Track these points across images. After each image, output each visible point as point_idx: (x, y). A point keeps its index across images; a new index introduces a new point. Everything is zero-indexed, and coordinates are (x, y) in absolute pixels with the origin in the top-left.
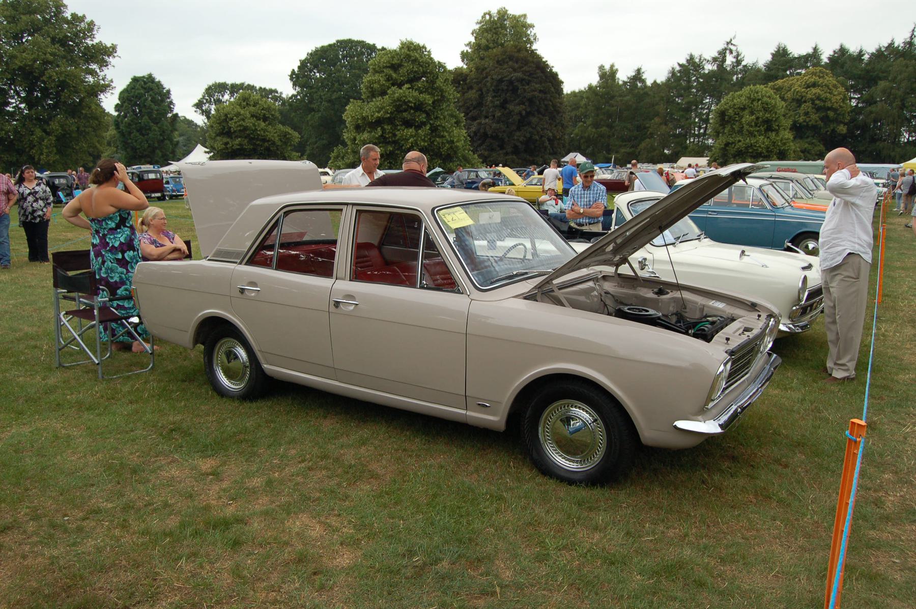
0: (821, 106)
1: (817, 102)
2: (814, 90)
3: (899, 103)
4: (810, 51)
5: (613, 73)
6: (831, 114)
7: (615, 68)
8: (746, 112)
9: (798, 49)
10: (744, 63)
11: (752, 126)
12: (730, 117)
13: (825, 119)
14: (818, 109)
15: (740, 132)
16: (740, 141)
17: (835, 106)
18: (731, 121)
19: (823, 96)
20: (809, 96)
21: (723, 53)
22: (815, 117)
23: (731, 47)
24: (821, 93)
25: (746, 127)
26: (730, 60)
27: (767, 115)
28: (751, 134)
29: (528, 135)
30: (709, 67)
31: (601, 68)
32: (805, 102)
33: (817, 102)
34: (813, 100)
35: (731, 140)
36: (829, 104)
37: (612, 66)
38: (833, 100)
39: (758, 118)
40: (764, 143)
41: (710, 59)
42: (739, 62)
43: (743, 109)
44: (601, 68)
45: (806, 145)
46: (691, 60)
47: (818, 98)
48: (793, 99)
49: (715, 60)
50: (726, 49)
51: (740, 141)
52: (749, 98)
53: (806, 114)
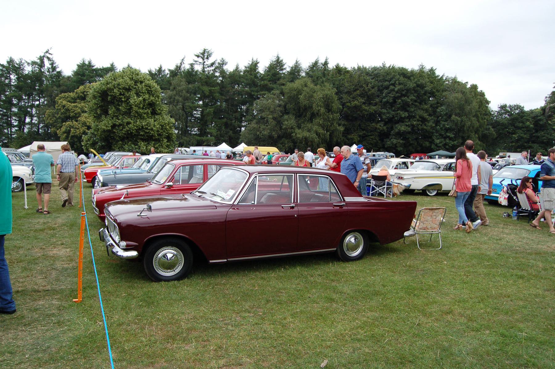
3: (181, 106)
4: (109, 66)
8: (132, 93)
9: (99, 63)
10: (58, 70)
11: (139, 108)
12: (114, 97)
15: (128, 113)
16: (128, 123)
18: (116, 101)
21: (41, 59)
23: (48, 55)
25: (135, 108)
26: (47, 64)
27: (152, 98)
28: (140, 116)
30: (28, 69)
35: (118, 122)
39: (144, 100)
40: (154, 126)
42: (54, 69)
43: (129, 90)
46: (11, 61)
49: (34, 63)
50: (44, 56)
51: (128, 123)
52: (132, 79)
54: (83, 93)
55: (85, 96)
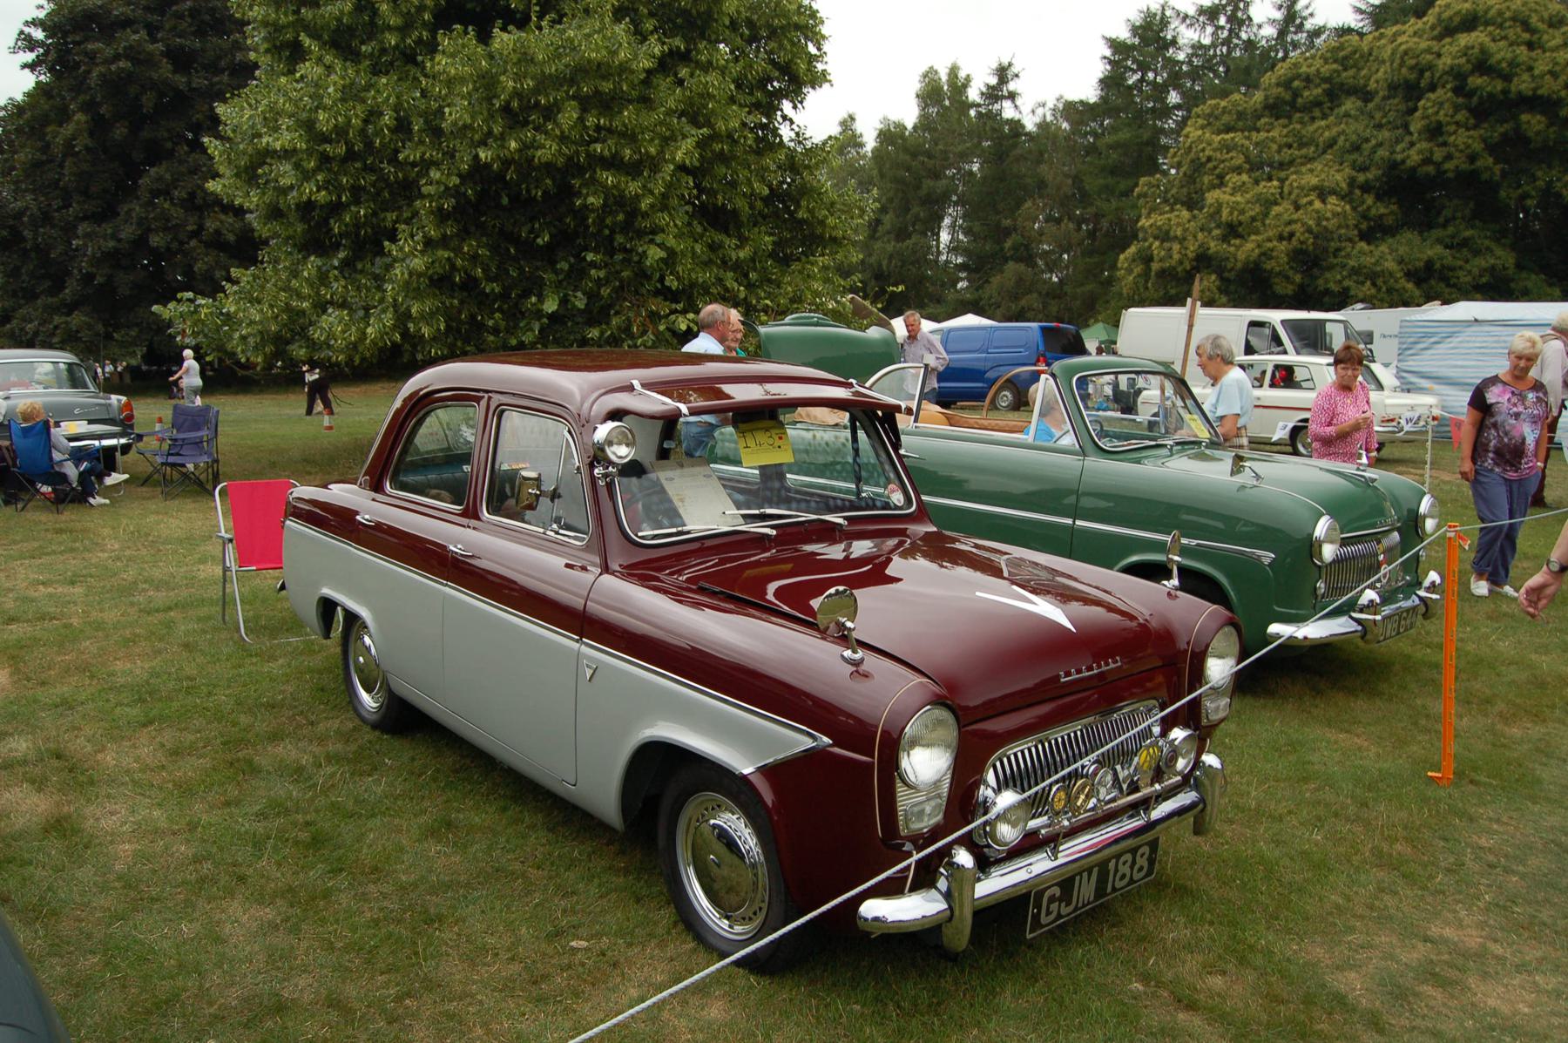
0: (1492, 100)
1: (1476, 81)
2: (1464, 39)
5: (959, 86)
6: (1533, 122)
7: (962, 74)
13: (1514, 148)
14: (1483, 110)
17: (1549, 87)
19: (1501, 53)
20: (1446, 61)
22: (1465, 139)
24: (1493, 47)
29: (128, 232)
31: (930, 76)
32: (1432, 88)
33: (1476, 81)
34: (1459, 78)
36: (1523, 84)
37: (953, 71)
38: (1541, 67)
41: (1192, 11)
44: (930, 76)
45: (1439, 249)
47: (1483, 65)
48: (1393, 88)
53: (1434, 131)
54: (1286, 84)
55: (1296, 94)
